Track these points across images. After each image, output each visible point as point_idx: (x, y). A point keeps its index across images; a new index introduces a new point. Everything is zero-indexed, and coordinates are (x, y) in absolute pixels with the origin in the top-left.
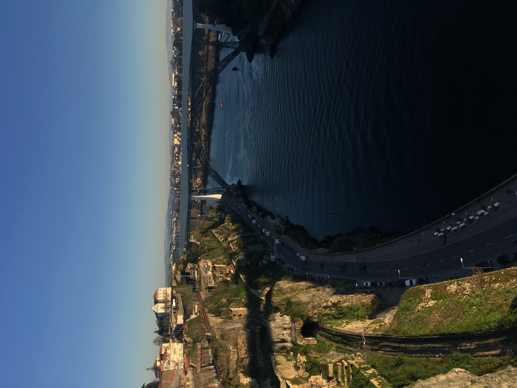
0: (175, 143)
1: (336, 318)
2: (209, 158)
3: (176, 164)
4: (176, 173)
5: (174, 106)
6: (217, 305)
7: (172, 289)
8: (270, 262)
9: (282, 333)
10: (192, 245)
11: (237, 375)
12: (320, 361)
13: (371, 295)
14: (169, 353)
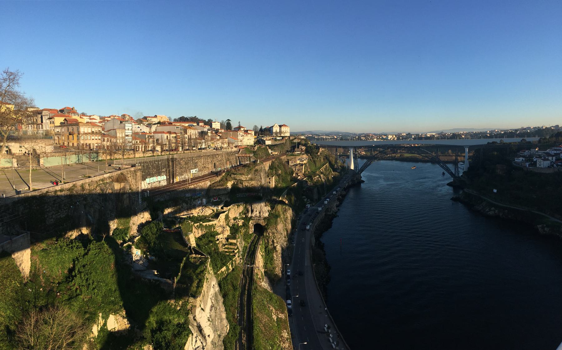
1: (265, 248)
6: (277, 167)
7: (289, 137)
8: (306, 204)
9: (257, 210)
10: (317, 149)
11: (233, 179)
12: (238, 234)
13: (281, 274)
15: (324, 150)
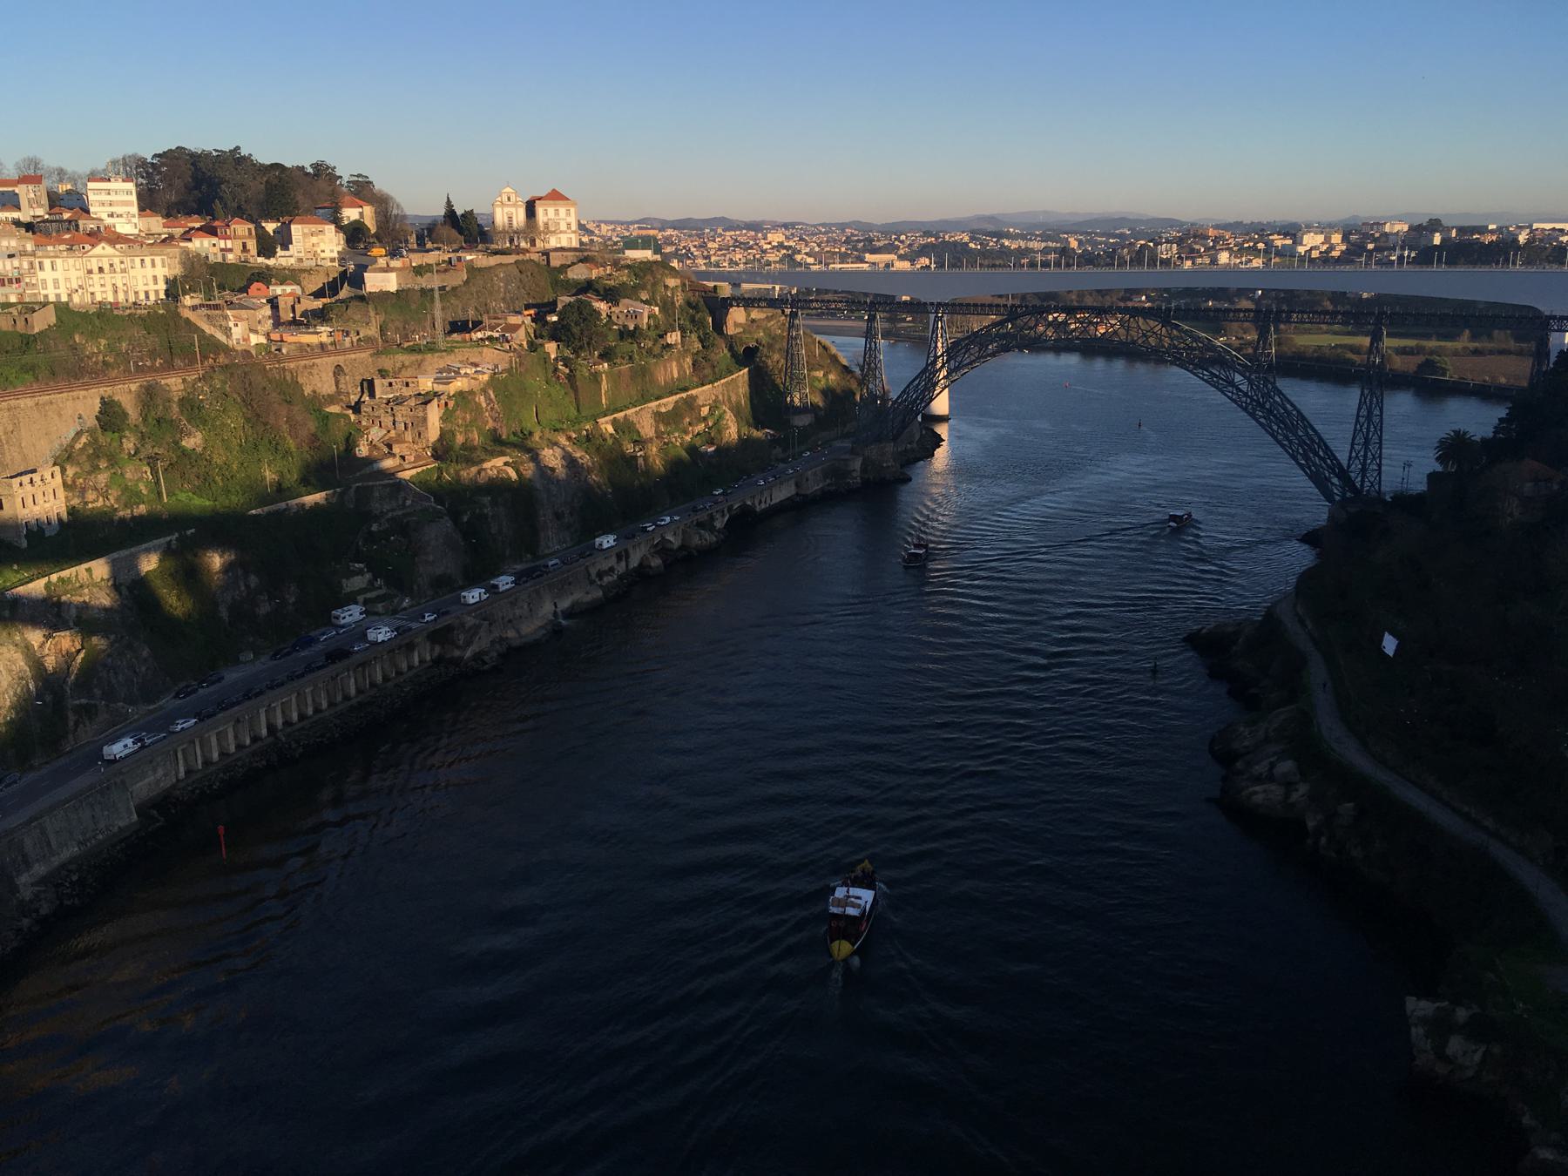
0: (1306, 238)
2: (1160, 361)
3: (1230, 244)
4: (1196, 243)
5: (1445, 230)
14: (90, 253)
15: (763, 316)
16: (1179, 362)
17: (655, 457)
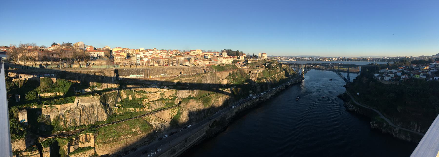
16: (331, 70)
17: (278, 80)
